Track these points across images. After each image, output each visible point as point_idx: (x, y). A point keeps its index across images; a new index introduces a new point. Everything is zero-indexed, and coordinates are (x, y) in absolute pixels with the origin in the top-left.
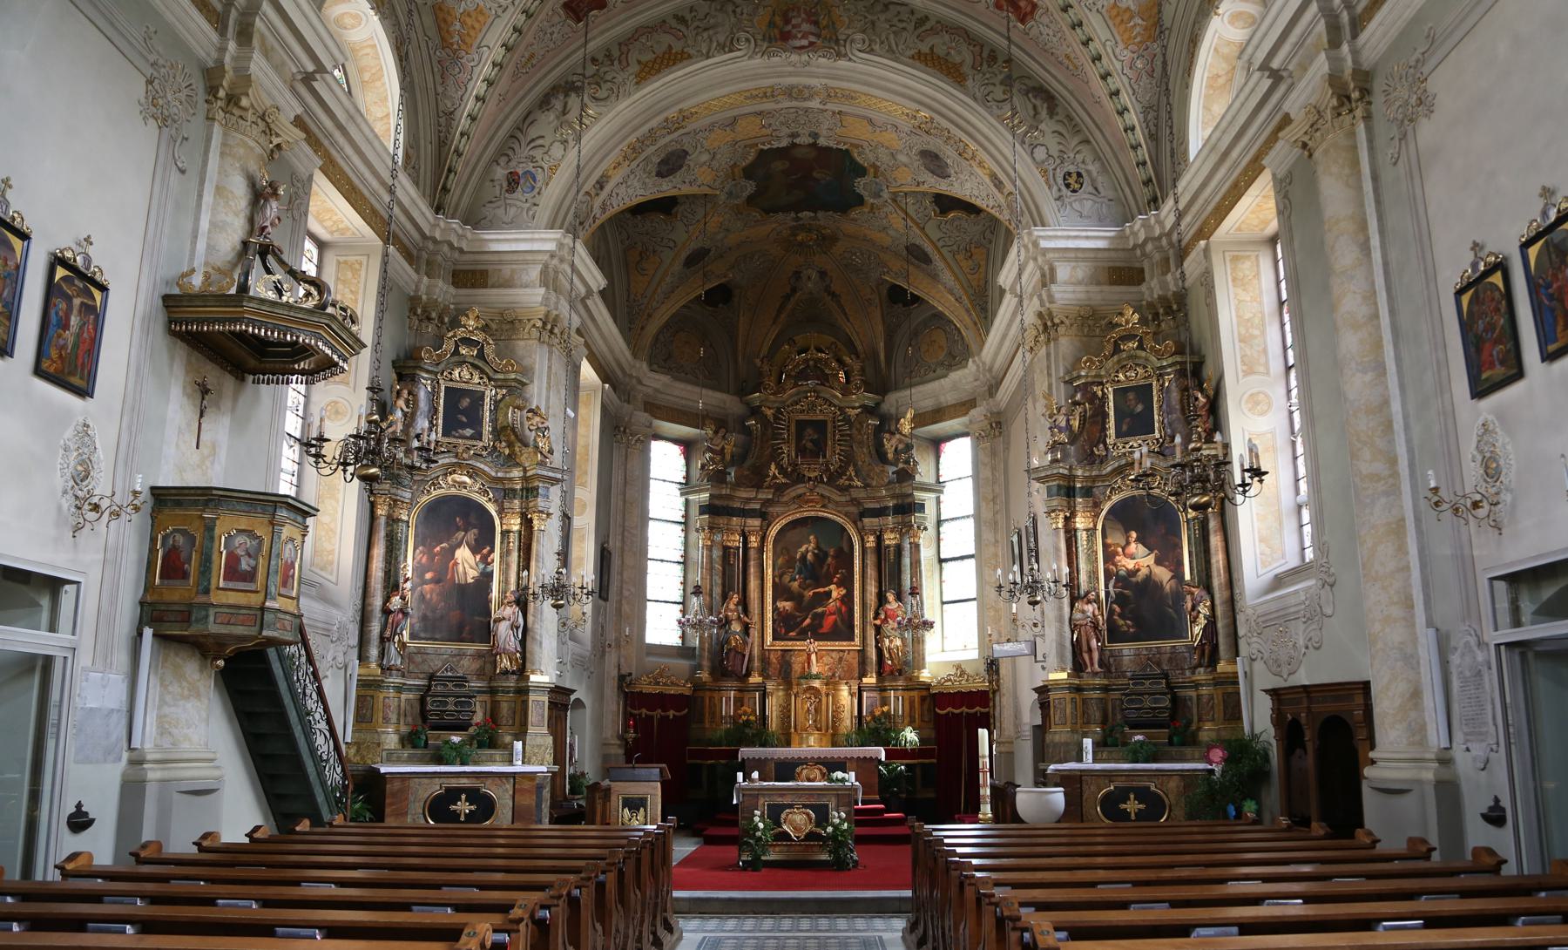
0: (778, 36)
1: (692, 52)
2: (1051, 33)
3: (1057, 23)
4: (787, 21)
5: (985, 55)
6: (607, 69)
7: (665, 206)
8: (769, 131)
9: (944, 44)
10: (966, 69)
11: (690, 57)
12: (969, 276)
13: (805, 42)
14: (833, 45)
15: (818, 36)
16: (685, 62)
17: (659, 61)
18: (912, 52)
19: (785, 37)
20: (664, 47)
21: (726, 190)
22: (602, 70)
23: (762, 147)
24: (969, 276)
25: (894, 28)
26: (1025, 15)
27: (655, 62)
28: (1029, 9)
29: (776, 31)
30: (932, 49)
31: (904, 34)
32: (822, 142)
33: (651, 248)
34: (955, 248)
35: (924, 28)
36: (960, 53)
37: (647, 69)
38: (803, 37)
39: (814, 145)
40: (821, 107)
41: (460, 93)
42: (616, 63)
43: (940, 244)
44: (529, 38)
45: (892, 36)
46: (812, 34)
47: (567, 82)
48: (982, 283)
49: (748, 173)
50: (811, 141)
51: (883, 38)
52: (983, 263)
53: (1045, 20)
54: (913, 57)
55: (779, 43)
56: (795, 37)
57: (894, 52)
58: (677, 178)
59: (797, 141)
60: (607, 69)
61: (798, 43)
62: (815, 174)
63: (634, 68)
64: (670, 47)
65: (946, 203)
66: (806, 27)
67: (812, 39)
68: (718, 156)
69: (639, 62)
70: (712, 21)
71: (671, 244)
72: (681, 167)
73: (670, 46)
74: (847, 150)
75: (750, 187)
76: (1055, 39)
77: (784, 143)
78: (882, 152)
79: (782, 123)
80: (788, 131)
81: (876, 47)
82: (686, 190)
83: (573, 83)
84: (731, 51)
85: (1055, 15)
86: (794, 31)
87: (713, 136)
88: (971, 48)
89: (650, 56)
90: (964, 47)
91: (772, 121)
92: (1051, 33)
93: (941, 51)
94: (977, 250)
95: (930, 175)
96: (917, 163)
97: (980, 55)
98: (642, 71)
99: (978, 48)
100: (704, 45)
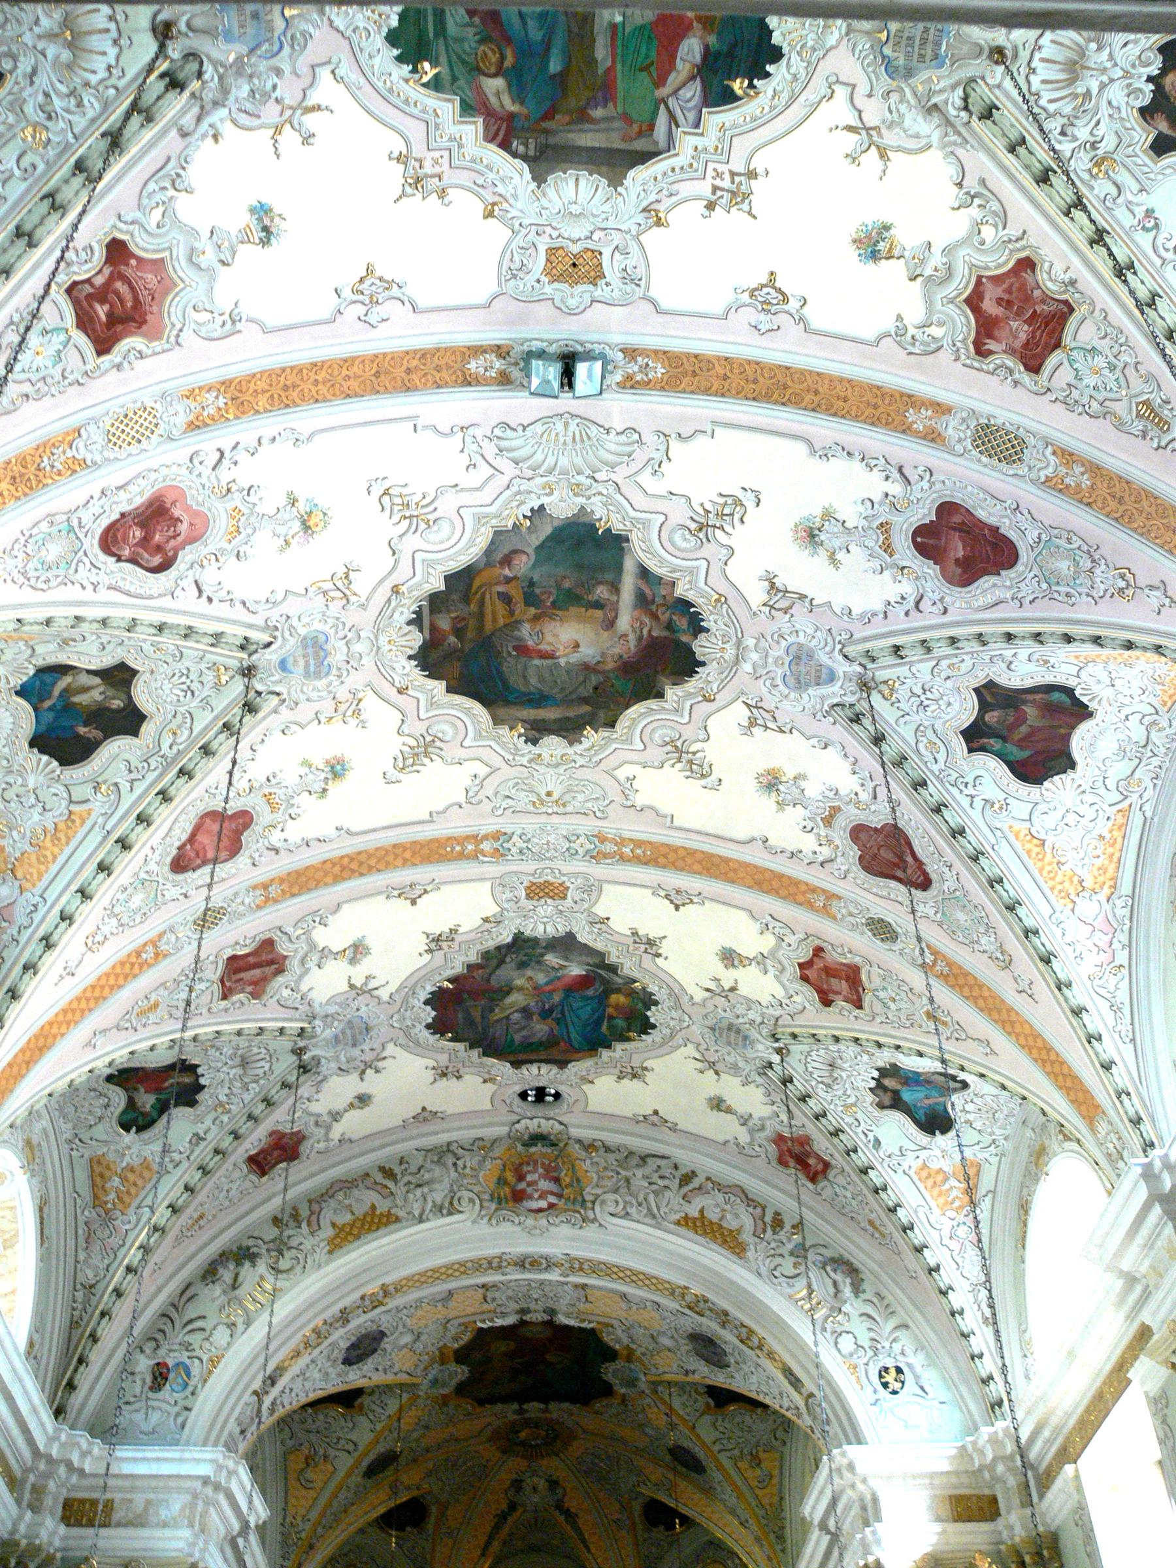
0: (509, 1196)
1: (401, 1214)
2: (849, 1195)
3: (856, 1185)
4: (521, 1178)
5: (768, 1219)
6: (291, 1232)
7: (348, 1399)
8: (491, 1307)
9: (717, 1205)
10: (747, 1236)
11: (398, 1220)
12: (757, 1491)
13: (543, 1204)
14: (578, 1208)
15: (560, 1196)
16: (392, 1227)
17: (358, 1224)
18: (677, 1217)
19: (519, 1197)
20: (366, 1208)
21: (430, 1377)
22: (286, 1233)
23: (480, 1325)
24: (757, 1491)
25: (654, 1187)
26: (816, 1173)
27: (352, 1225)
28: (820, 1167)
29: (507, 1190)
30: (702, 1211)
31: (668, 1194)
32: (562, 1319)
33: (321, 1451)
34: (737, 1452)
35: (691, 1186)
36: (737, 1216)
37: (342, 1235)
38: (541, 1197)
39: (550, 1324)
40: (561, 1279)
41: (107, 1262)
42: (304, 1225)
43: (717, 1447)
44: (201, 1197)
45: (651, 1197)
46: (552, 1193)
47: (240, 1248)
48: (776, 1499)
49: (461, 1356)
50: (546, 1317)
51: (641, 1198)
52: (776, 1472)
53: (841, 1180)
54: (678, 1223)
55: (511, 1204)
56: (531, 1197)
57: (654, 1217)
58: (368, 1365)
59: (527, 1318)
60: (291, 1232)
61: (535, 1205)
62: (548, 1357)
63: (327, 1232)
64: (373, 1207)
65: (722, 1398)
66: (544, 1185)
67: (552, 1199)
68: (423, 1338)
69: (334, 1225)
70: (427, 1176)
71: (351, 1447)
72: (374, 1351)
73: (373, 1207)
74: (593, 1330)
75: (461, 1372)
76: (854, 1203)
77: (511, 1320)
78: (638, 1332)
79: (510, 1298)
80: (517, 1307)
81: (633, 1211)
82: (379, 1378)
83: (248, 1248)
84: (450, 1214)
85: (853, 1175)
86: (529, 1190)
87: (420, 1313)
88: (751, 1210)
89: (346, 1218)
90: (742, 1209)
91: (497, 1295)
92: (849, 1195)
93: (713, 1215)
94: (767, 1455)
95: (703, 1362)
96: (686, 1346)
97: (762, 1220)
98: (337, 1236)
99: (759, 1210)
100: (416, 1205)
